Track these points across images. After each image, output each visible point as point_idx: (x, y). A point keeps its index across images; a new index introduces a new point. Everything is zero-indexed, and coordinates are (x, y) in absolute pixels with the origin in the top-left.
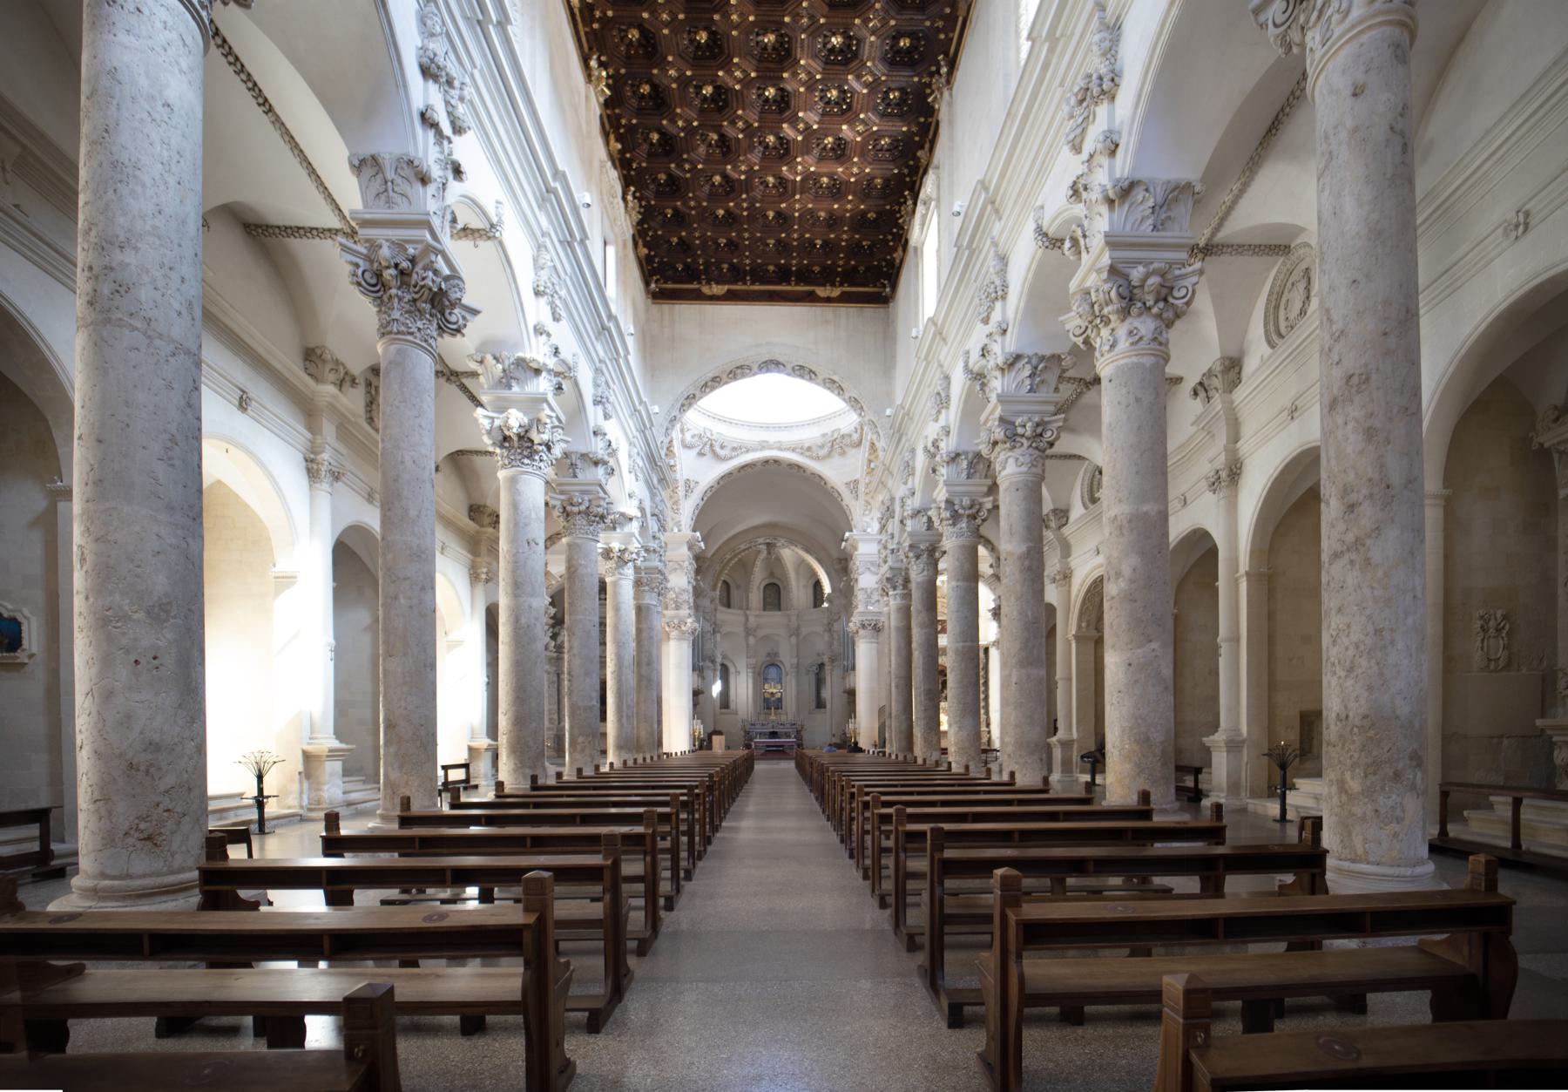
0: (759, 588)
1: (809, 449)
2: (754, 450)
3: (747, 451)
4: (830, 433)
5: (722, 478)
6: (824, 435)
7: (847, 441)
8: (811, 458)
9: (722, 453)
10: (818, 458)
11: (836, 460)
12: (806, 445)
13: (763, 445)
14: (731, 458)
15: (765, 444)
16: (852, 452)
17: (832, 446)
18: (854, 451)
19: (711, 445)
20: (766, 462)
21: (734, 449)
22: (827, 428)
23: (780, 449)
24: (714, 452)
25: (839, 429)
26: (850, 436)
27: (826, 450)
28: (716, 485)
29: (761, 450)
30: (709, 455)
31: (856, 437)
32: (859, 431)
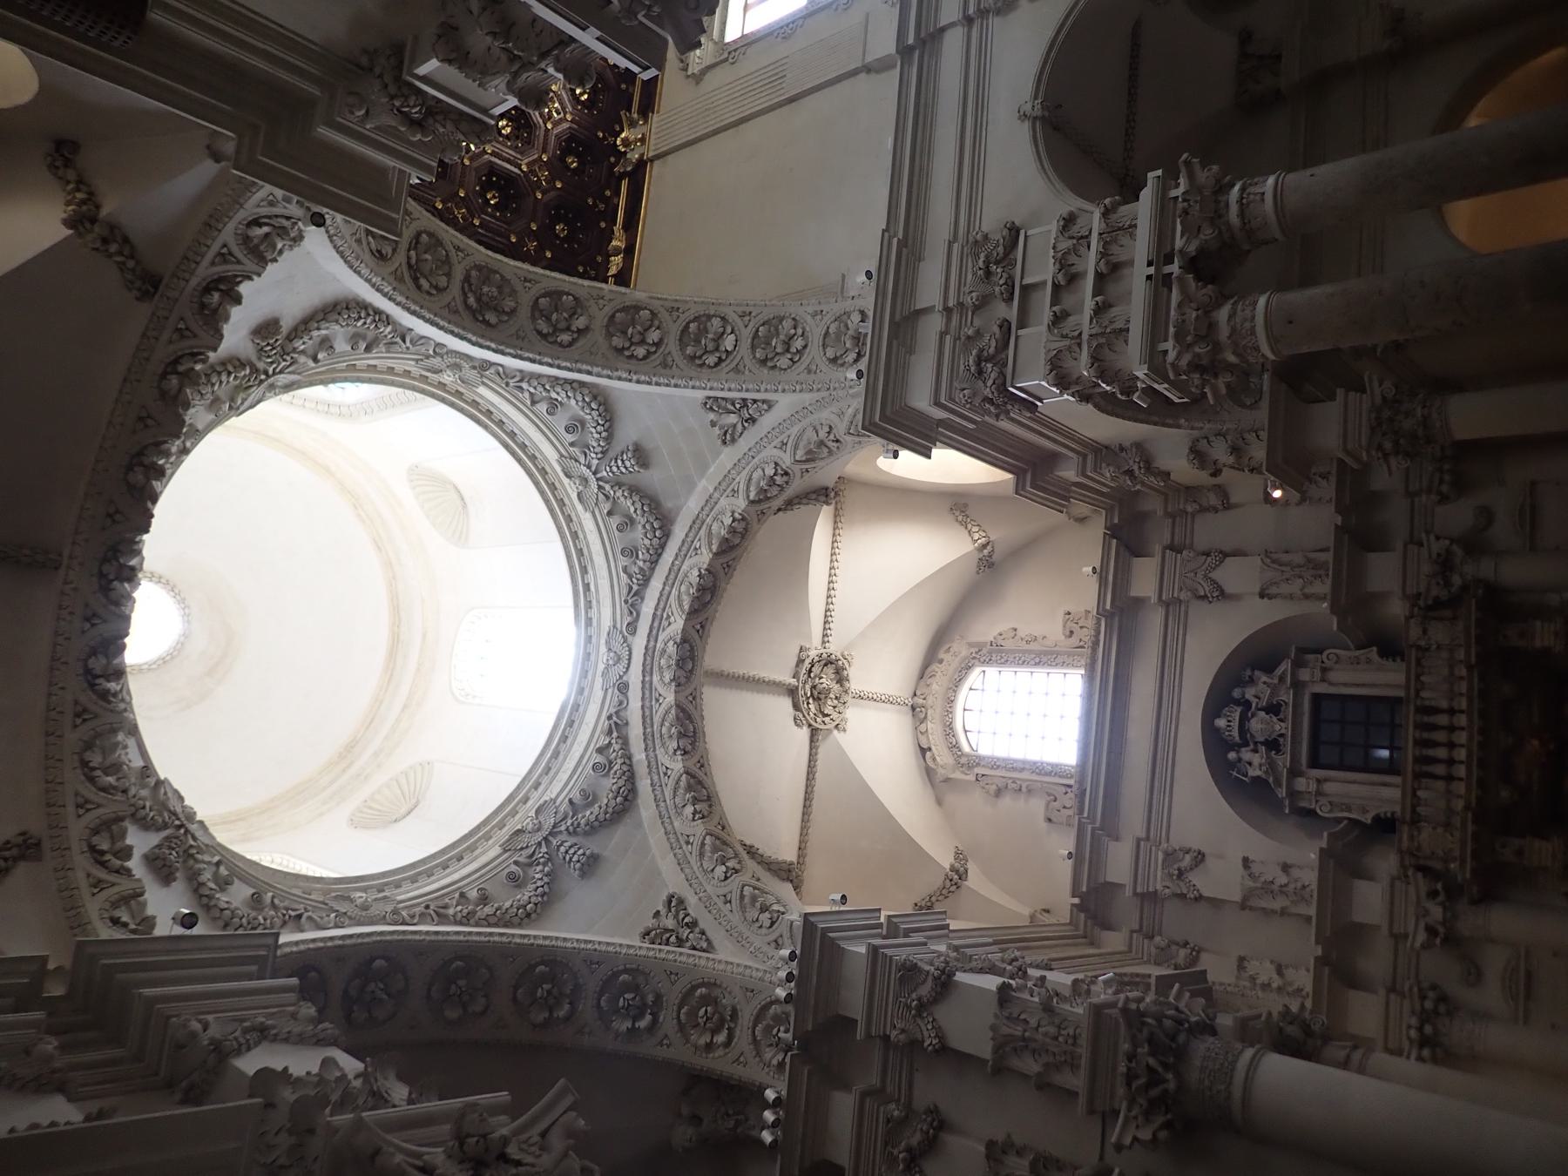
12: (473, 894)
16: (611, 844)
31: (608, 784)
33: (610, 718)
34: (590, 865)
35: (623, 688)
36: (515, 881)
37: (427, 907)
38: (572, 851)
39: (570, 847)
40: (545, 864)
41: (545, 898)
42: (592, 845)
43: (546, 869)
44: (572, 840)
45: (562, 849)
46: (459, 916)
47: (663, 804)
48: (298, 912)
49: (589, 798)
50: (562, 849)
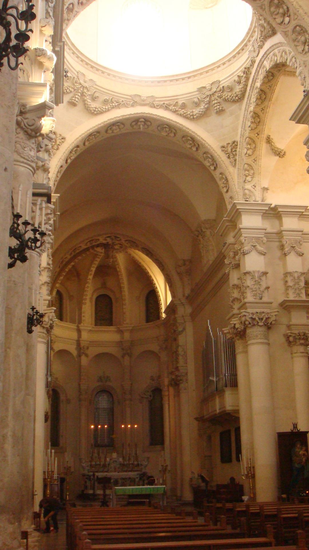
0: (91, 299)
1: (184, 106)
2: (126, 106)
3: (119, 105)
4: (208, 87)
5: (91, 135)
6: (201, 90)
7: (227, 94)
8: (186, 117)
9: (93, 105)
10: (192, 118)
11: (213, 119)
12: (180, 103)
13: (135, 101)
14: (101, 113)
15: (137, 99)
17: (209, 102)
18: (234, 107)
19: (83, 94)
20: (136, 120)
21: (106, 102)
22: (206, 82)
23: (153, 106)
24: (84, 101)
25: (220, 82)
26: (230, 89)
27: (202, 106)
28: (81, 145)
29: (132, 106)
30: (80, 105)
31: (238, 89)
32: (243, 80)
33: (245, 68)
34: (221, 112)
35: (253, 62)
36: (197, 105)
37: (164, 103)
38: (216, 105)
39: (217, 103)
40: (206, 104)
41: (202, 115)
42: (225, 105)
43: (206, 106)
44: (219, 100)
45: (214, 102)
46: (172, 110)
47: (246, 112)
48: (119, 103)
49: (231, 89)
50: (214, 102)
